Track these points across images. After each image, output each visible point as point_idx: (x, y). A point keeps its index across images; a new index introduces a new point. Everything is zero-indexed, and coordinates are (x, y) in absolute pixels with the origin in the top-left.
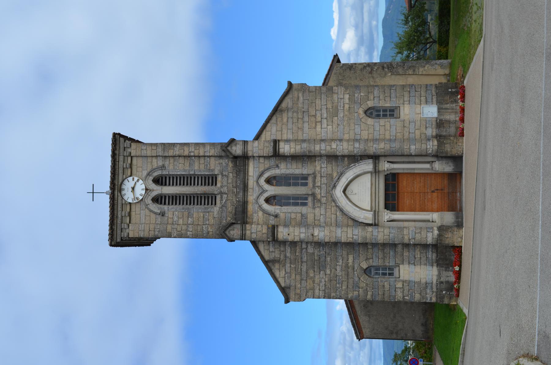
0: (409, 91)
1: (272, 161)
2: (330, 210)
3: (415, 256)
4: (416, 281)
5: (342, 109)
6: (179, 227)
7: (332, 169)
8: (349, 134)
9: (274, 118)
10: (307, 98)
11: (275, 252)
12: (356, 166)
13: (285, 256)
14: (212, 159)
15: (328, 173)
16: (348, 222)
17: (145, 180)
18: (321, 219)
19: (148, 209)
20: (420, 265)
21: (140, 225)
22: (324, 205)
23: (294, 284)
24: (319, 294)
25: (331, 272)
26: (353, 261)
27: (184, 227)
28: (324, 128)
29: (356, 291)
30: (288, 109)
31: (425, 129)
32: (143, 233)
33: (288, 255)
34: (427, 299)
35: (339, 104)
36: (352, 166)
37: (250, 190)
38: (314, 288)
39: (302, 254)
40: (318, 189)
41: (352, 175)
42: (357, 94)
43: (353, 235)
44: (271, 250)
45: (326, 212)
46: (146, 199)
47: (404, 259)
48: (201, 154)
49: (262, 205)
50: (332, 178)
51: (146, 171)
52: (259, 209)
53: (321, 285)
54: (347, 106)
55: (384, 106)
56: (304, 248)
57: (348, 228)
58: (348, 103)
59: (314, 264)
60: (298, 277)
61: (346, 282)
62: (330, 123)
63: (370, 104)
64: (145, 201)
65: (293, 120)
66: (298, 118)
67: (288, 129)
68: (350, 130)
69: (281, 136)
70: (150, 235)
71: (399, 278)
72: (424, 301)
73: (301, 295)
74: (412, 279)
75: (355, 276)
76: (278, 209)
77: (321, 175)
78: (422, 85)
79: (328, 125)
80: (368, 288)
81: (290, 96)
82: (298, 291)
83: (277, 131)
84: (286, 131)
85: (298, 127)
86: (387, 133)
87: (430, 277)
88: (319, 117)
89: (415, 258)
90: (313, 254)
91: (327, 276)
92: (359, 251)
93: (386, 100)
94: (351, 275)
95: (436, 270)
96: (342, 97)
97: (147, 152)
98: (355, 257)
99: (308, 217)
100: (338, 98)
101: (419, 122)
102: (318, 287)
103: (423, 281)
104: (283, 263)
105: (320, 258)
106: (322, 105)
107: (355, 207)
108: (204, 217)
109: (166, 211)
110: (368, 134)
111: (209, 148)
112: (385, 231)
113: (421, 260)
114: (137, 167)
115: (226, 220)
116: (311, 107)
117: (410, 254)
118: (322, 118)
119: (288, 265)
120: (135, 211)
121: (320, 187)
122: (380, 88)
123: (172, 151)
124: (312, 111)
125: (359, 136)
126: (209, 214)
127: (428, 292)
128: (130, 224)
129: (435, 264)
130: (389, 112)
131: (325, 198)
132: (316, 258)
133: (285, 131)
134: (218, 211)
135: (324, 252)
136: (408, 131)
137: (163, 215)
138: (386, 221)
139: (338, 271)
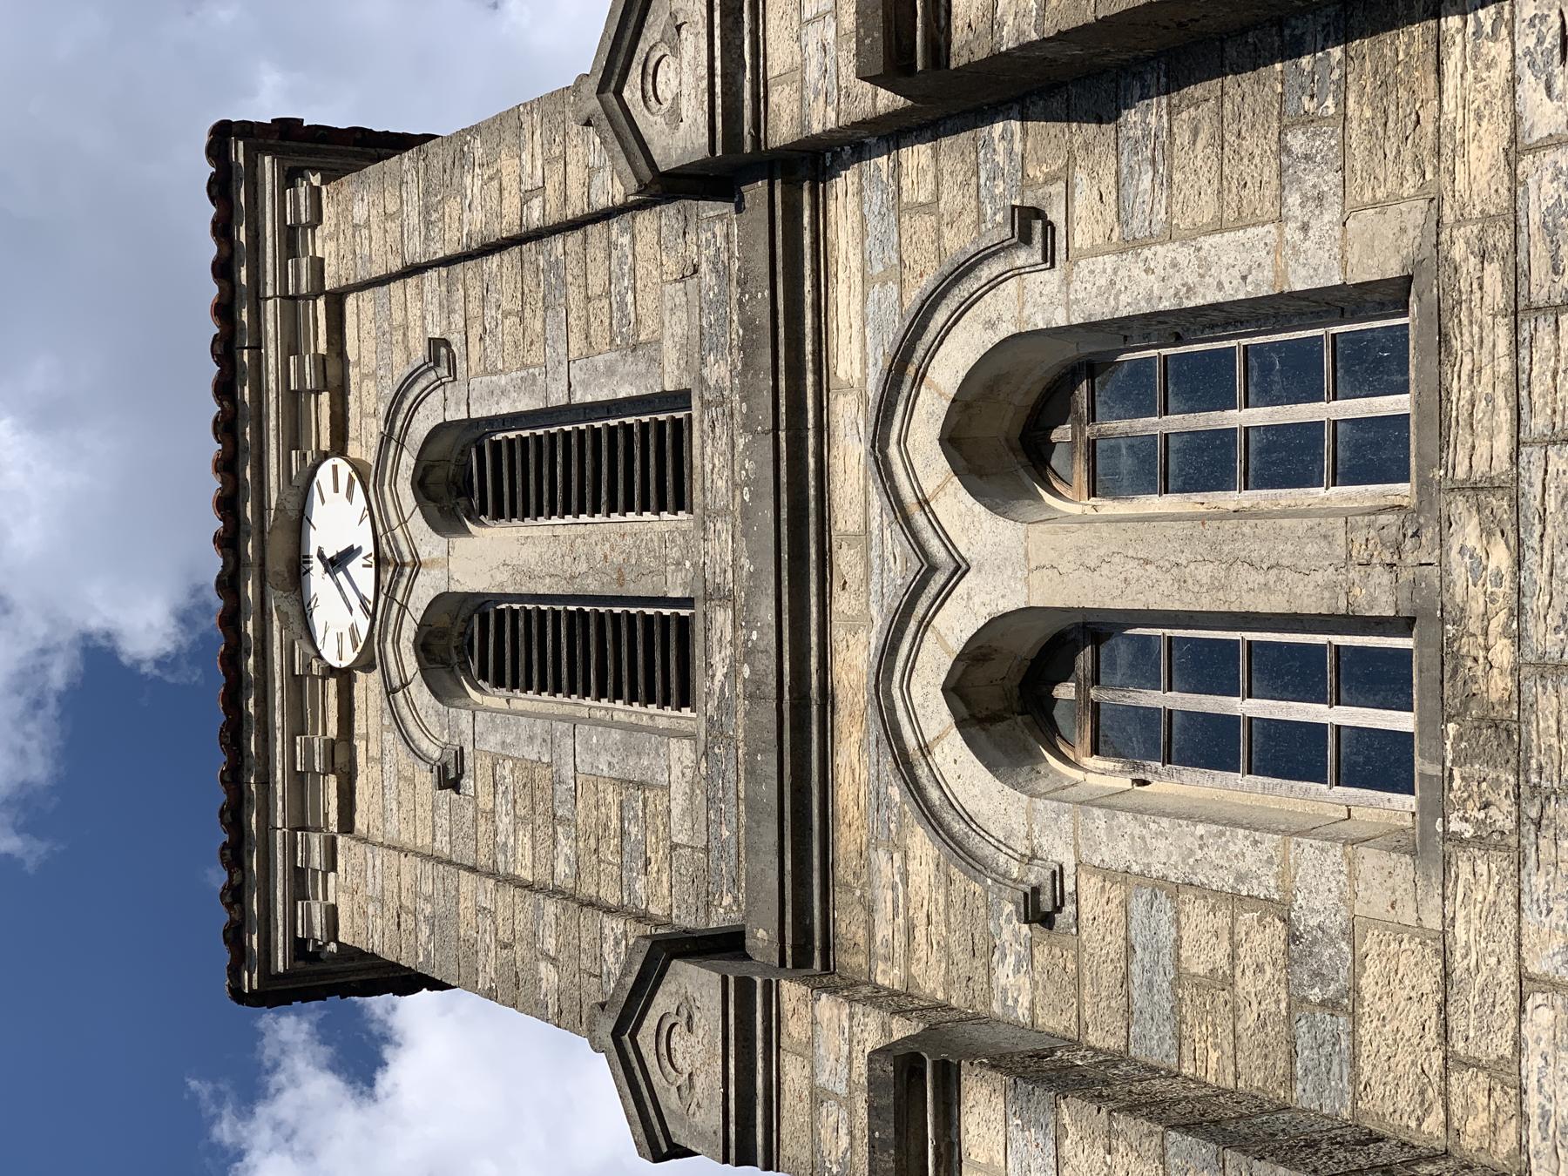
18: (1532, 1063)
40: (1486, 532)
77: (1517, 276)
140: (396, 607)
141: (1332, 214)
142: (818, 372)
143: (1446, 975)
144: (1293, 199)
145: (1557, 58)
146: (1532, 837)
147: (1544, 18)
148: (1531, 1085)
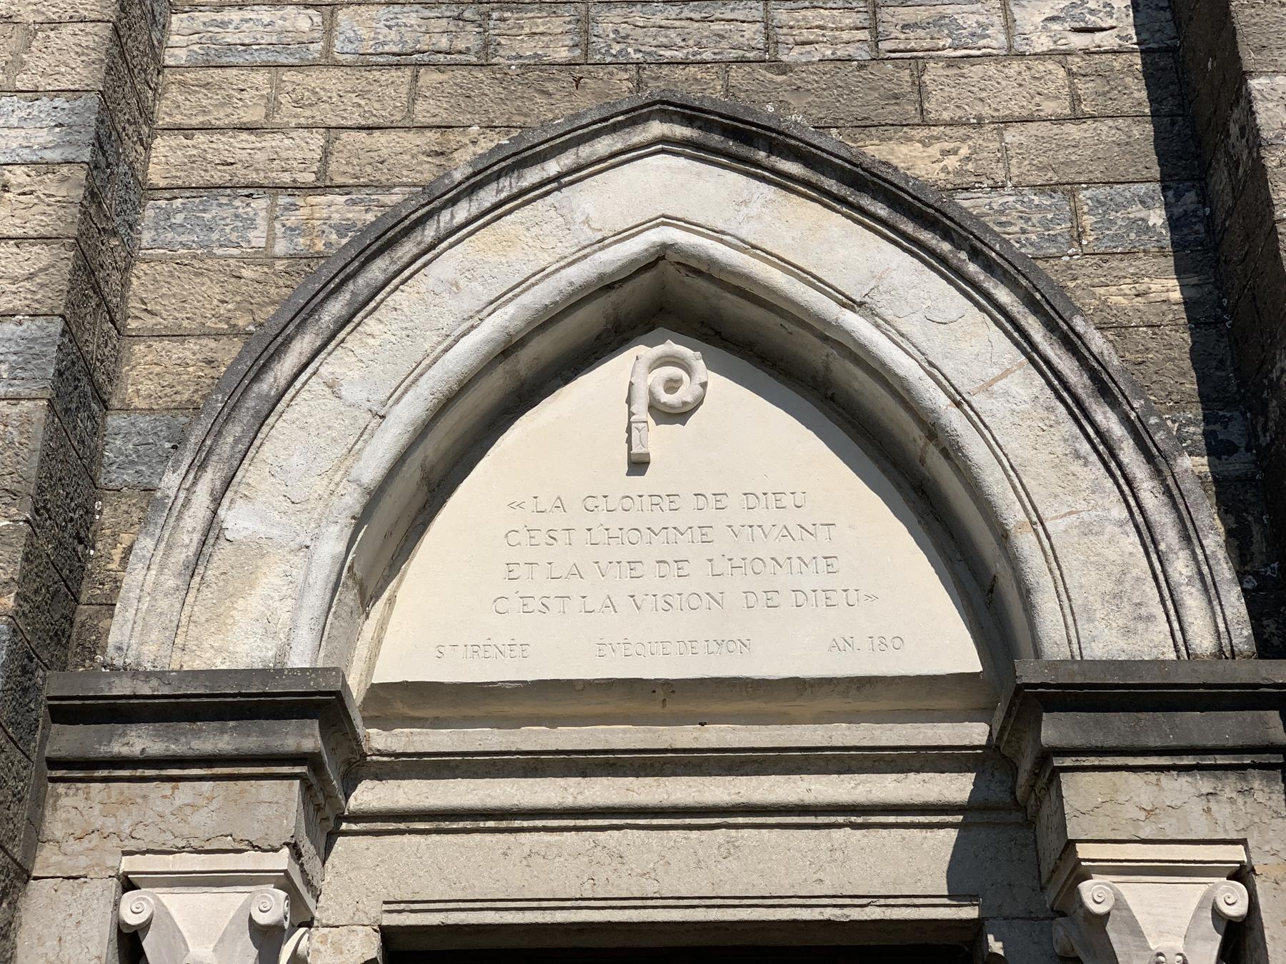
2: (381, 113)
7: (1007, 122)
12: (1079, 413)
15: (934, 72)
16: (180, 336)
36: (1072, 343)
41: (931, 368)
45: (365, 64)
50: (864, 125)
131: (563, 54)
138: (133, 910)
145: (1077, 25)
146: (448, 14)
147: (1110, 15)
148: (247, 14)
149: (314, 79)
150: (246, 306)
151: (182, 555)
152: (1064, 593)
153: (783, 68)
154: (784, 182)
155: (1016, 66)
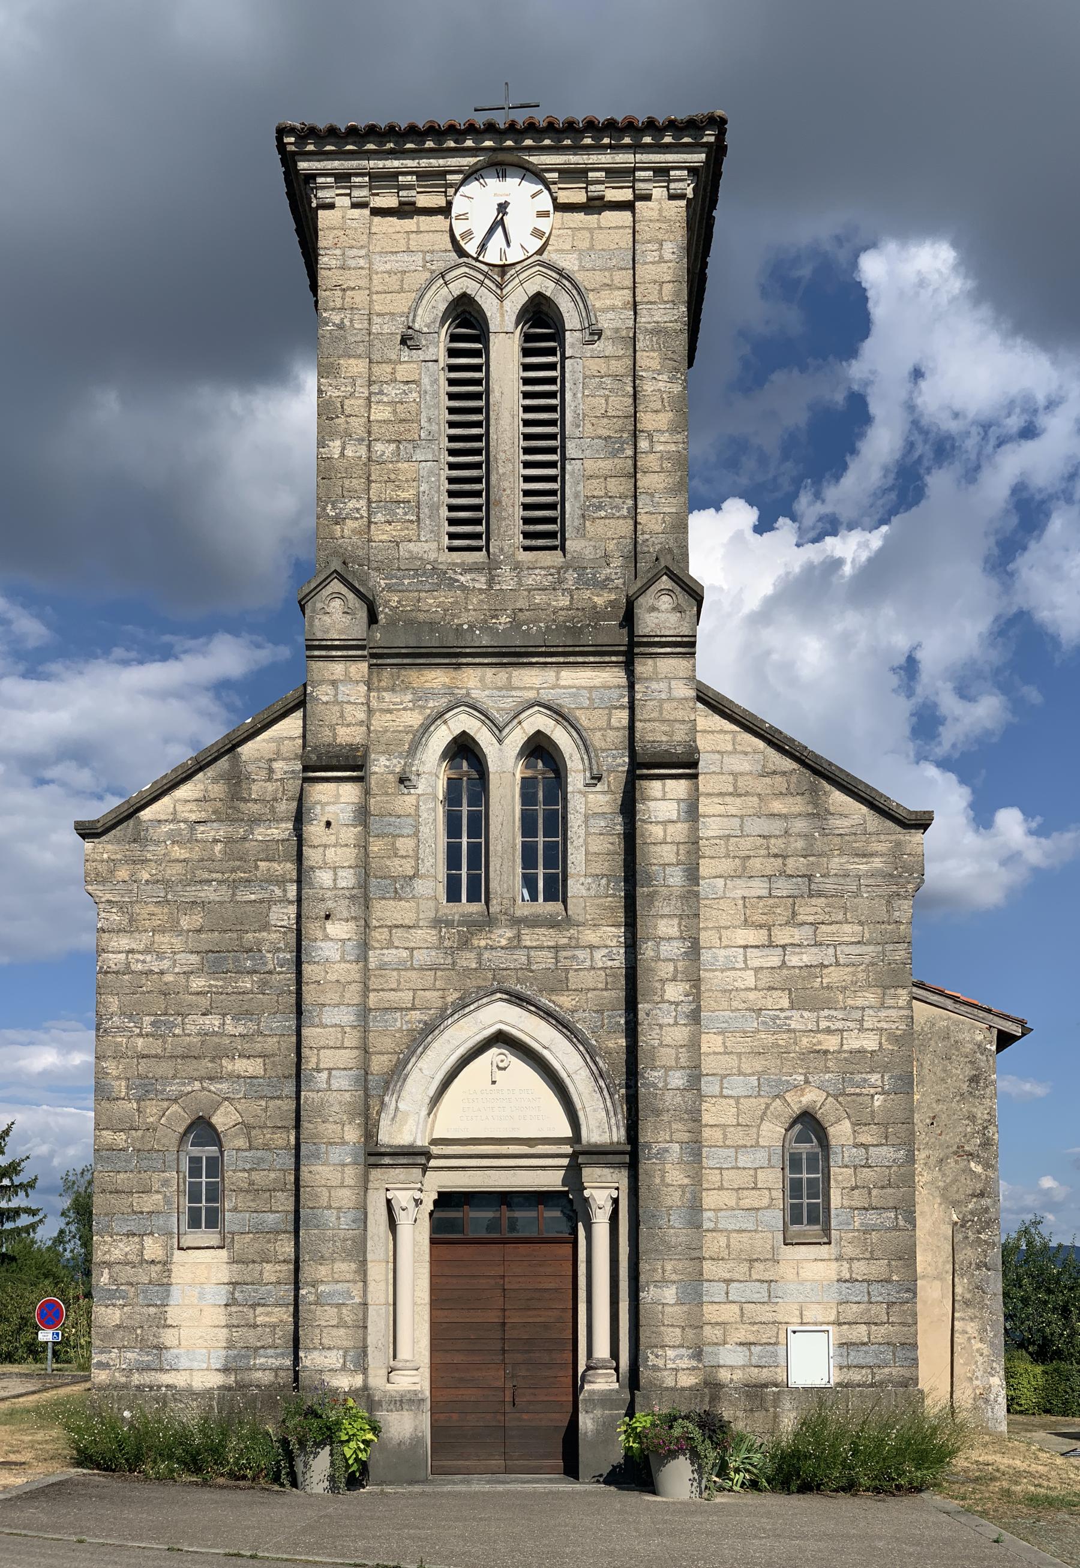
0: (888, 1281)
1: (614, 757)
2: (428, 985)
3: (264, 1305)
4: (166, 1309)
5: (823, 1024)
6: (359, 406)
8: (726, 1053)
9: (788, 764)
10: (863, 888)
11: (269, 779)
12: (596, 1081)
13: (255, 821)
14: (625, 527)
15: (571, 973)
16: (383, 1054)
17: (540, 259)
18: (394, 951)
19: (431, 282)
20: (227, 1326)
21: (363, 252)
22: (449, 961)
23: (149, 856)
24: (113, 952)
25: (198, 993)
26: (239, 1077)
27: (357, 425)
28: (745, 956)
29: (127, 1087)
30: (819, 814)
31: (743, 1340)
32: (333, 263)
33: (260, 833)
34: (101, 1353)
35: (840, 1014)
36: (596, 1063)
37: (503, 674)
38: (137, 930)
39: (265, 885)
40: (509, 939)
41: (563, 1067)
42: (879, 1083)
43: (330, 1070)
44: (277, 765)
46: (467, 270)
47: (251, 1266)
48: (644, 481)
49: (445, 722)
51: (576, 268)
52: (428, 711)
53: (148, 958)
54: (831, 1043)
55: (832, 1182)
56: (285, 891)
57: (356, 1053)
58: (845, 1047)
59: (225, 931)
60: (174, 872)
61: (159, 1051)
62: (765, 979)
63: (840, 1132)
64: (458, 266)
65: (776, 837)
66: (785, 857)
67: (742, 817)
68: (739, 1054)
69: (716, 791)
70: (328, 293)
71: (180, 1249)
72: (97, 1342)
73: (109, 887)
74: (175, 1291)
75: (184, 1084)
76: (435, 788)
77: (564, 947)
78: (912, 1329)
79: (757, 970)
80: (140, 1133)
81: (873, 821)
82: (123, 873)
83: (735, 775)
84: (734, 812)
85: (749, 857)
86: (727, 1198)
87: (184, 1363)
88: (792, 936)
89: (253, 1306)
90: (265, 927)
91: (182, 979)
92: (278, 1098)
93: (856, 1192)
94: (191, 1068)
95: (209, 1385)
96: (866, 1025)
97: (652, 263)
98: (255, 1081)
99: (403, 903)
100: (863, 1009)
101: (768, 1317)
102: (141, 947)
103: (168, 1337)
104: (230, 811)
105: (251, 950)
106: (835, 947)
107: (440, 1077)
108: (399, 502)
109: (420, 355)
110: (724, 1127)
111: (667, 510)
112: (346, 1193)
113: (245, 1329)
114: (591, 230)
115: (389, 588)
116: (828, 905)
117: (269, 1287)
118: (784, 947)
119: (221, 831)
120: (418, 232)
121: (515, 944)
122: (903, 1170)
123: (655, 364)
124: (813, 910)
125: (716, 1090)
126: (412, 522)
127: (129, 1355)
128: (367, 212)
129: (231, 1380)
130: (802, 1204)
131: (474, 966)
132: (250, 935)
133: (735, 805)
134: (421, 559)
135: (270, 967)
136: (737, 1276)
137: (404, 341)
138: (390, 1195)
139: (201, 1020)
140: (481, 277)
141: (584, 893)
142: (564, 663)
143: (410, 927)
144: (590, 880)
149: (409, 974)
150: (397, 1045)
151: (391, 1116)
152: (588, 1126)
153: (532, 971)
154: (530, 1011)
155: (593, 972)
